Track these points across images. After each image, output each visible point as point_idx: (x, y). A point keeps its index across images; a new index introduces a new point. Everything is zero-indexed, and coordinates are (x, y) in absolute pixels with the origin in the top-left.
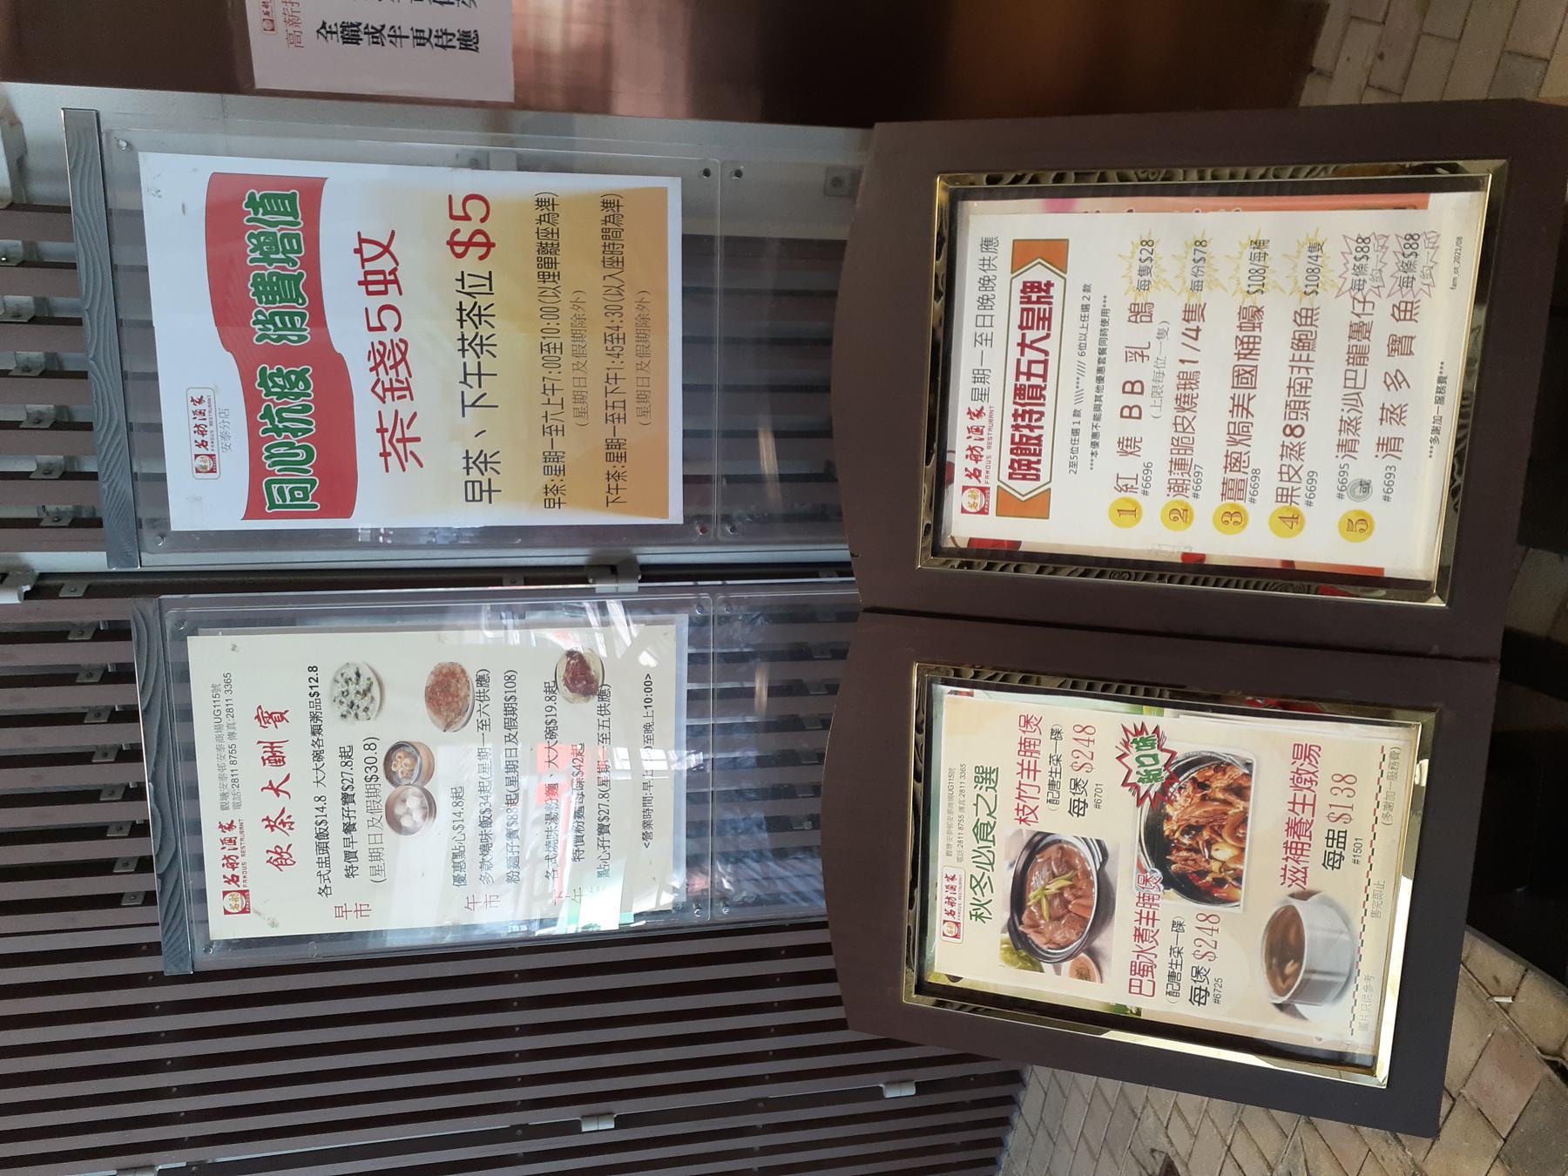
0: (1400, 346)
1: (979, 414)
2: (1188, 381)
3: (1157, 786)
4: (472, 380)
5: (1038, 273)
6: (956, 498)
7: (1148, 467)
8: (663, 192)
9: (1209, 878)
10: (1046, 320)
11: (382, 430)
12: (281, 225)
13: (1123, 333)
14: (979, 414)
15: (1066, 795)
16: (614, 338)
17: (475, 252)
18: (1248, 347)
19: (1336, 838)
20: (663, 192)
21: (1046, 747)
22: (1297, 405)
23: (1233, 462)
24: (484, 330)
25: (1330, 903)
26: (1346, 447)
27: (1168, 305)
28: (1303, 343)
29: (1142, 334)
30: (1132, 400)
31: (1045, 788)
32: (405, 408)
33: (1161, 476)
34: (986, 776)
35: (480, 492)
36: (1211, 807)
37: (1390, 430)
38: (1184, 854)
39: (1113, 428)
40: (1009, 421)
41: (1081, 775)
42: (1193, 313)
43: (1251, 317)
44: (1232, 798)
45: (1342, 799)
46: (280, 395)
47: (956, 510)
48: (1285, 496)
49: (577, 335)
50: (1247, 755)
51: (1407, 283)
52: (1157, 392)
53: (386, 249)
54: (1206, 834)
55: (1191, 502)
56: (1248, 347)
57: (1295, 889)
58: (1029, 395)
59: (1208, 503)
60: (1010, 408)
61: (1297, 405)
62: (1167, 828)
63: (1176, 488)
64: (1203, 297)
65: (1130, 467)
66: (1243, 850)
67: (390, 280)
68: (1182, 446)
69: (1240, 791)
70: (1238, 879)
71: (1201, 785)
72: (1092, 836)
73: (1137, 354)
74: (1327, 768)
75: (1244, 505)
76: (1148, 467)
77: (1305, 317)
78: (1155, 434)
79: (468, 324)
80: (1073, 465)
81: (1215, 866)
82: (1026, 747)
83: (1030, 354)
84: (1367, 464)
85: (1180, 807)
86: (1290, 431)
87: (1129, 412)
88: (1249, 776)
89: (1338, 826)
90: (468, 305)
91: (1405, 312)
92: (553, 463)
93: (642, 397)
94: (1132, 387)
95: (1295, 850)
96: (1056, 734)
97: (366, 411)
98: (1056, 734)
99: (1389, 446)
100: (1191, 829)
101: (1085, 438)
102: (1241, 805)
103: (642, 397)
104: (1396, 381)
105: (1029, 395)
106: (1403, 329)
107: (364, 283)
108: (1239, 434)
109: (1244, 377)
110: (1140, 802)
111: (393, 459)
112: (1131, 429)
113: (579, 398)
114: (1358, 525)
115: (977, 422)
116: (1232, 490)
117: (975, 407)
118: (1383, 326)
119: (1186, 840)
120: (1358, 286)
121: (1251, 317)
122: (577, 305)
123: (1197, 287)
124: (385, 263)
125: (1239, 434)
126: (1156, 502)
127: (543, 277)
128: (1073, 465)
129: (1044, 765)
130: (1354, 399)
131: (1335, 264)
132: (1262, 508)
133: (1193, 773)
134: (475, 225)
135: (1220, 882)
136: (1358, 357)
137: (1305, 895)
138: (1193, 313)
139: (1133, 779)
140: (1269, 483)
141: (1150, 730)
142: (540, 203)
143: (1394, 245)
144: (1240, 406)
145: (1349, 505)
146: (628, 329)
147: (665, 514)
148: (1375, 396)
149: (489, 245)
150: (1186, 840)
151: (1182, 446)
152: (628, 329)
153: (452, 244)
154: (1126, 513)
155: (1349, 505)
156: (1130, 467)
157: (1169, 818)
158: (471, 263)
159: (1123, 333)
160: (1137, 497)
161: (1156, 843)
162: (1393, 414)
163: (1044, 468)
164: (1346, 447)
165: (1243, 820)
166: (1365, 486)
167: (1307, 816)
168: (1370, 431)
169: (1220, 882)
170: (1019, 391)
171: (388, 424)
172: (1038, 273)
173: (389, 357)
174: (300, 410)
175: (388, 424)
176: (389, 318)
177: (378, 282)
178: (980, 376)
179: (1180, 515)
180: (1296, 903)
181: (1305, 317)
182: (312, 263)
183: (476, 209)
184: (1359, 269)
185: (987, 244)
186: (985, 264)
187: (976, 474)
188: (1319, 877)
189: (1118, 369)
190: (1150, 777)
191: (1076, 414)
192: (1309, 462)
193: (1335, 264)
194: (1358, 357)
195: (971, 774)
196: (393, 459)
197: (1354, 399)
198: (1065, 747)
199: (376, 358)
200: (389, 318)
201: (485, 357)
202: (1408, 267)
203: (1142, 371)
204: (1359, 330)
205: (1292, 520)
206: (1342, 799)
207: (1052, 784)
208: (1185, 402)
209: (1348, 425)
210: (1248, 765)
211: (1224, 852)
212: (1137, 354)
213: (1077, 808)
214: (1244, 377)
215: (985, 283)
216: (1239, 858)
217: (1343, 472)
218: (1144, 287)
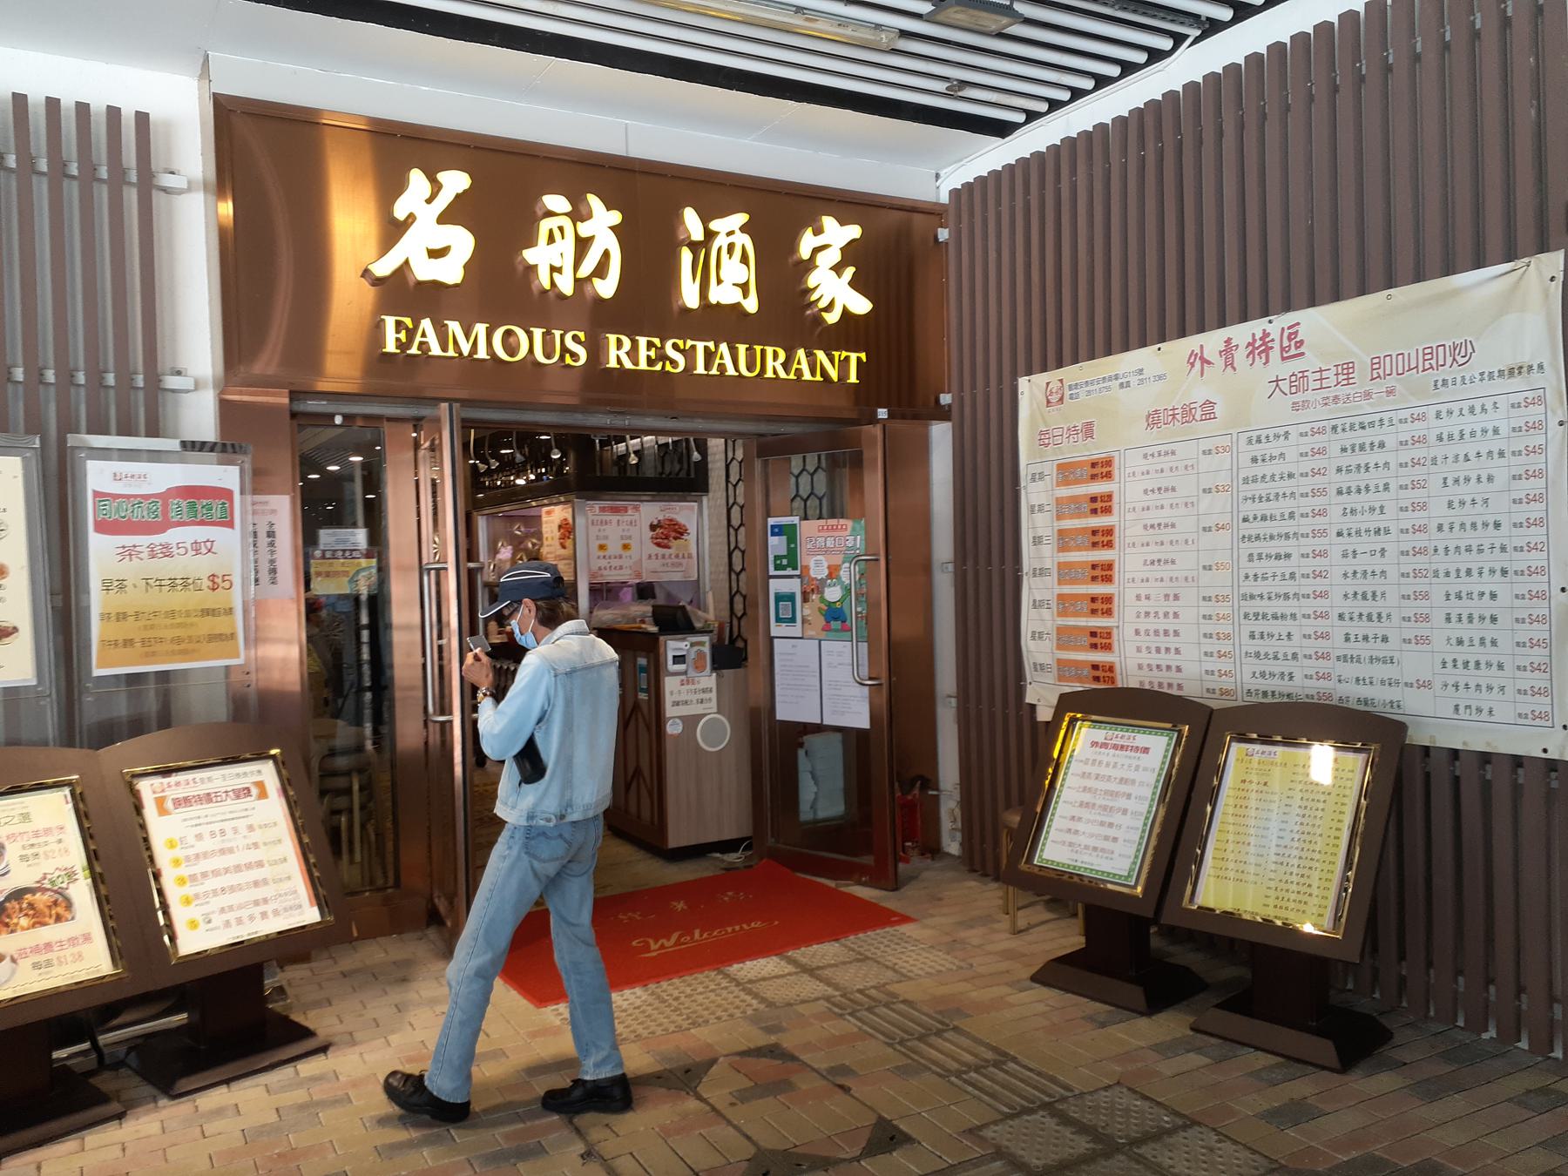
0: (264, 915)
1: (195, 783)
2: (231, 851)
3: (49, 886)
4: (158, 583)
5: (254, 791)
6: (157, 781)
7: (193, 846)
8: (238, 656)
9: (7, 920)
10: (238, 797)
11: (135, 546)
12: (217, 514)
13: (242, 824)
14: (195, 783)
15: (30, 852)
16: (179, 640)
17: (210, 584)
18: (249, 866)
19: (49, 964)
20: (238, 656)
21: (51, 839)
22: (232, 889)
23: (204, 875)
24: (179, 588)
25: (13, 972)
26: (222, 910)
27: (256, 836)
28: (256, 884)
29: (244, 831)
30: (218, 833)
31: (30, 842)
32: (145, 555)
33: (191, 852)
34: (26, 817)
35: (107, 586)
36: (47, 911)
37: (233, 922)
38: (17, 906)
39: (205, 830)
40: (196, 793)
41: (42, 856)
42: (256, 845)
43: (260, 864)
44: (54, 917)
45: (70, 959)
46: (149, 509)
47: (152, 782)
48: (197, 896)
49: (179, 625)
50: (78, 917)
51: (286, 910)
52: (223, 841)
53: (209, 551)
54: (31, 912)
55: (183, 865)
56: (249, 866)
57: (16, 956)
58: (208, 798)
59: (185, 871)
60: (201, 793)
61: (232, 889)
62: (28, 896)
63: (187, 859)
64: (263, 847)
65: (191, 840)
66: (28, 929)
67: (197, 552)
68: (205, 855)
69: (59, 919)
70: (12, 932)
71: (55, 903)
72: (11, 867)
73: (235, 830)
74: (84, 948)
75: (188, 884)
76: (193, 846)
77: (265, 882)
78: (208, 844)
79: (181, 581)
80: (185, 820)
81: (15, 921)
82: (48, 831)
83: (224, 795)
84: (218, 920)
85: (41, 899)
86: (223, 890)
87: (213, 834)
88: (67, 920)
89: (55, 962)
90: (190, 581)
91: (276, 913)
92: (122, 616)
93: (154, 653)
94: (223, 832)
95: (36, 950)
96: (60, 841)
97: (143, 541)
98: (60, 841)
99: (227, 924)
100: (31, 906)
101: (198, 821)
102: (52, 921)
103: (154, 653)
104: (252, 918)
105: (208, 798)
106: (270, 914)
107: (196, 543)
108: (216, 873)
109: (238, 868)
110: (38, 882)
111: (121, 550)
112: (207, 835)
113: (152, 627)
114: (193, 925)
115: (191, 782)
116: (193, 878)
117: (197, 780)
118: (269, 908)
119: (25, 905)
120: (280, 895)
121: (260, 864)
122: (192, 625)
123: (265, 844)
124: (204, 550)
125: (216, 873)
126: (179, 853)
127: (202, 610)
128: (185, 820)
129: (41, 840)
130: (240, 907)
131: (285, 886)
132: (188, 890)
133: (61, 899)
134: (222, 585)
135: (7, 925)
136: (256, 903)
137: (14, 960)
138: (256, 845)
139: (49, 877)
140: (200, 889)
141: (76, 877)
142: (231, 609)
143: (297, 902)
144: (227, 871)
145: (200, 919)
146: (183, 646)
147: (99, 667)
148: (244, 913)
149: (214, 590)
150: (25, 905)
151: (205, 855)
152: (183, 646)
153: (213, 575)
154: (172, 845)
155: (200, 919)
156: (191, 840)
157: (34, 895)
158: (206, 583)
159: (242, 824)
160: (179, 847)
161: (18, 894)
162: (239, 921)
163: (177, 811)
164: (222, 910)
165: (44, 924)
166: (209, 922)
167: (56, 949)
168: (231, 916)
169: (7, 925)
170: (209, 794)
171: (138, 549)
172: (254, 791)
173: (167, 552)
174: (142, 514)
175: (138, 549)
176: (182, 551)
177: (197, 547)
178: (210, 779)
179: (177, 862)
180: (8, 959)
181: (265, 882)
182: (202, 523)
183: (227, 585)
184: (286, 894)
185: (259, 772)
186: (252, 772)
187: (169, 786)
188: (25, 964)
189: (227, 826)
190: (52, 882)
191: (206, 816)
192: (213, 900)
193: (285, 886)
194: (256, 903)
195: (24, 811)
196: (121, 550)
197: (240, 907)
198: (55, 846)
199: (166, 546)
200: (182, 551)
201: (168, 588)
202: (291, 908)
203: (230, 834)
204: (265, 901)
205: (187, 901)
206: (70, 959)
207: (32, 845)
208: (222, 852)
209: (231, 908)
210: (73, 919)
211: (24, 922)
212: (235, 830)
213: (23, 858)
214: (238, 868)
215: (245, 774)
216: (23, 929)
217: (213, 912)
218: (260, 827)
